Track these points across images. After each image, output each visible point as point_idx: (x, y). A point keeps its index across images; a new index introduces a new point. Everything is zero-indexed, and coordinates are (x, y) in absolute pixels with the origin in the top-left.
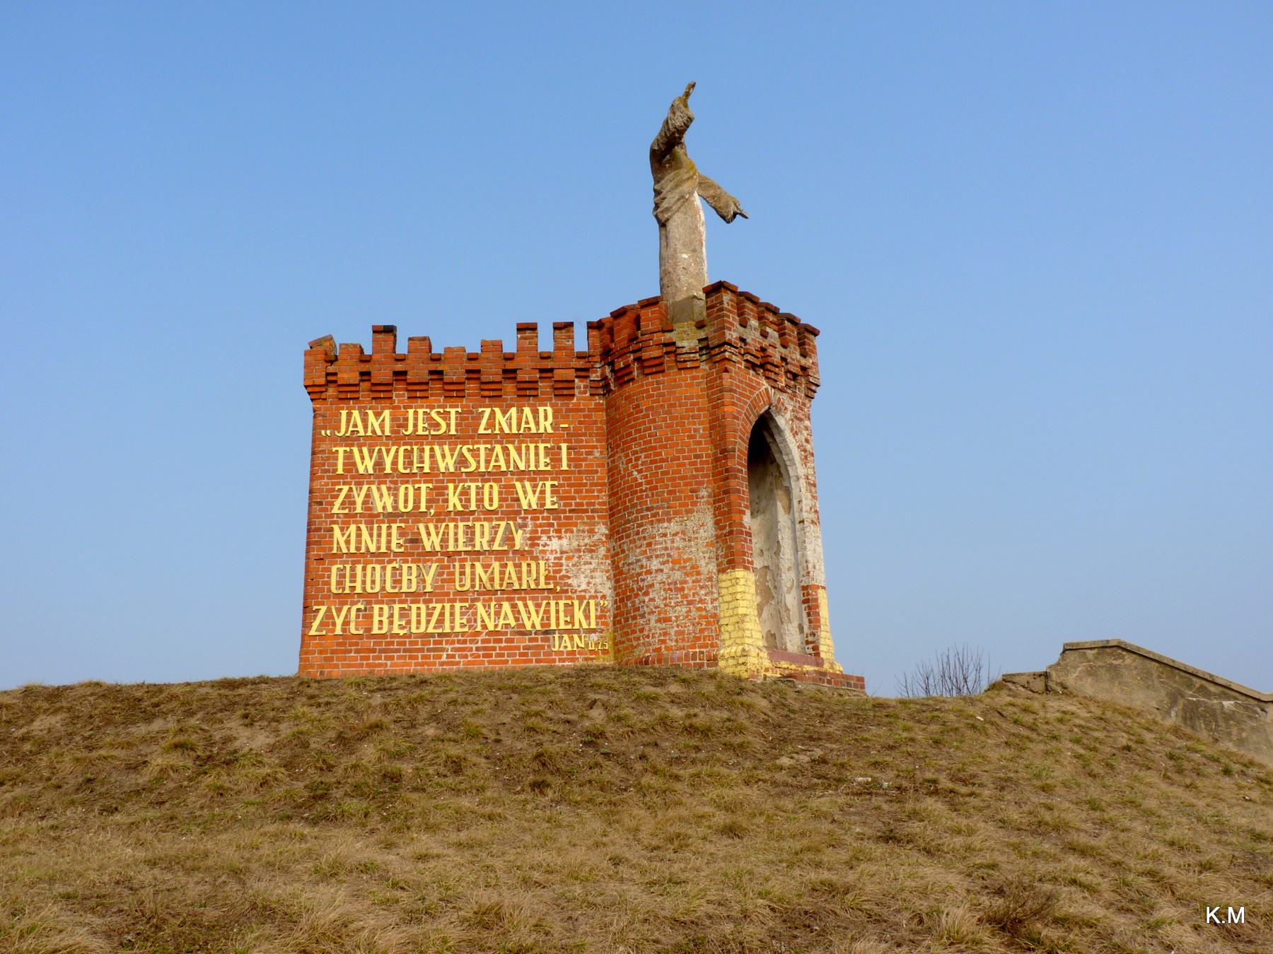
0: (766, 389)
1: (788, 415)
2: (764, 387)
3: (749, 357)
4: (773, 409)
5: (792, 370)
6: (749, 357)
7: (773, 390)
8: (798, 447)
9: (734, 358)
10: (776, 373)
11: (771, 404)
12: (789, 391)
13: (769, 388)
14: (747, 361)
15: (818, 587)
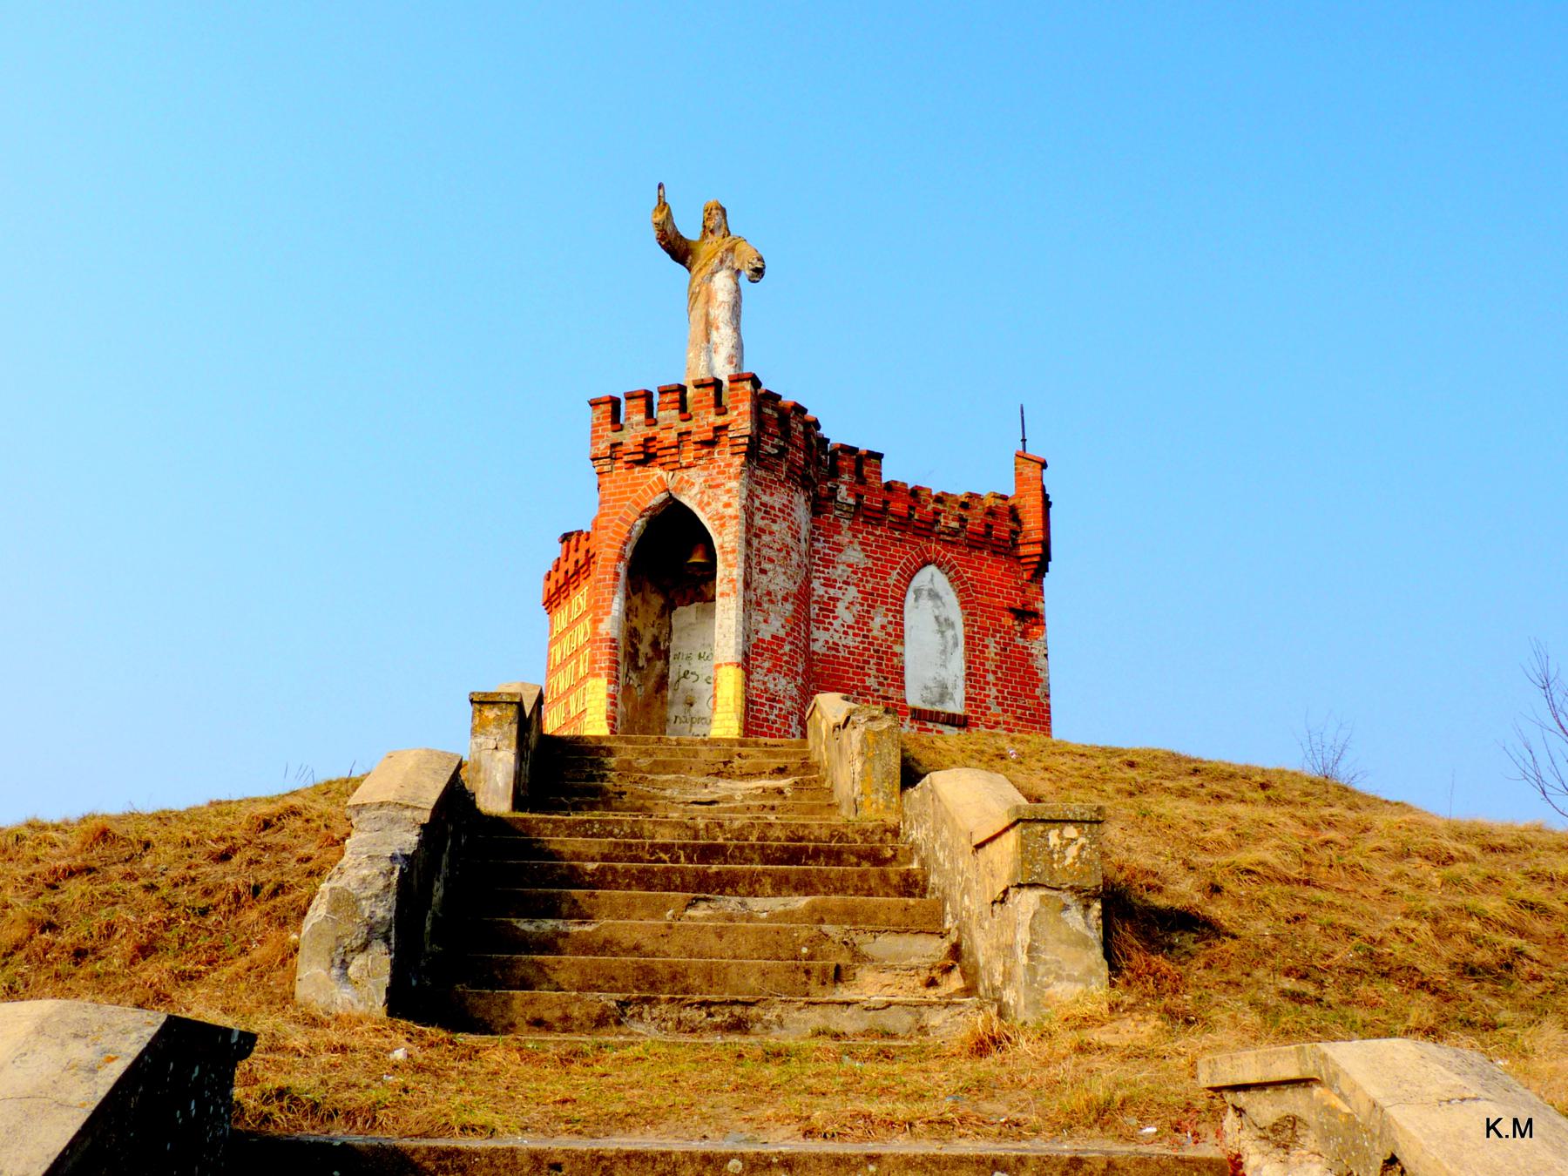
0: (660, 479)
1: (695, 490)
2: (655, 478)
3: (626, 458)
4: (673, 492)
5: (697, 439)
6: (626, 458)
7: (671, 473)
8: (709, 519)
9: (606, 468)
10: (671, 455)
11: (667, 490)
12: (701, 462)
13: (664, 475)
14: (627, 462)
15: (719, 666)
